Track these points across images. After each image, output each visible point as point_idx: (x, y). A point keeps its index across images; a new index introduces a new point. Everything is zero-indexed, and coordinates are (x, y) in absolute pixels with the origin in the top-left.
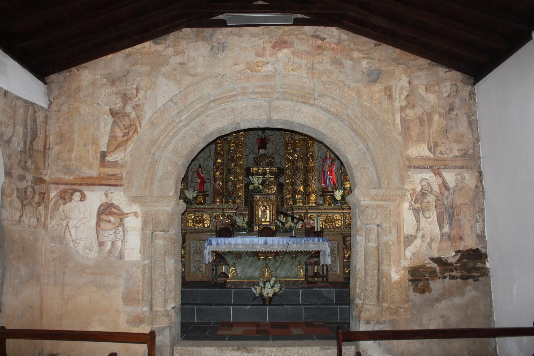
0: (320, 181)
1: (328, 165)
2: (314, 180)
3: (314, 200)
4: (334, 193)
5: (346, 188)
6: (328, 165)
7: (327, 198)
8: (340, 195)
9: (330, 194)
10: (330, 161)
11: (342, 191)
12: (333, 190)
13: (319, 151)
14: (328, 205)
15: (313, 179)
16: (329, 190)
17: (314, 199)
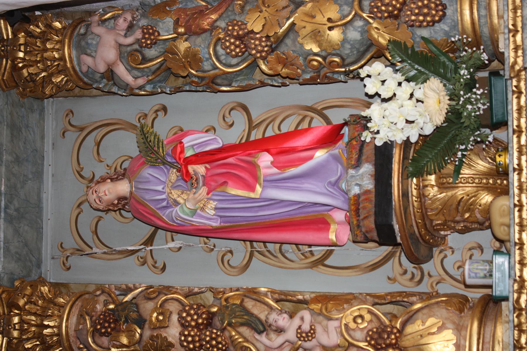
0: (319, 251)
1: (175, 194)
2: (282, 320)
3: (459, 329)
4: (388, 146)
5: (354, 35)
6: (175, 194)
7: (446, 204)
8: (407, 88)
9: (405, 176)
10: (148, 172)
11: (377, 67)
12: (368, 152)
13: (111, 252)
14: (503, 202)
15: (280, 331)
16: (369, 184)
17: (449, 334)
